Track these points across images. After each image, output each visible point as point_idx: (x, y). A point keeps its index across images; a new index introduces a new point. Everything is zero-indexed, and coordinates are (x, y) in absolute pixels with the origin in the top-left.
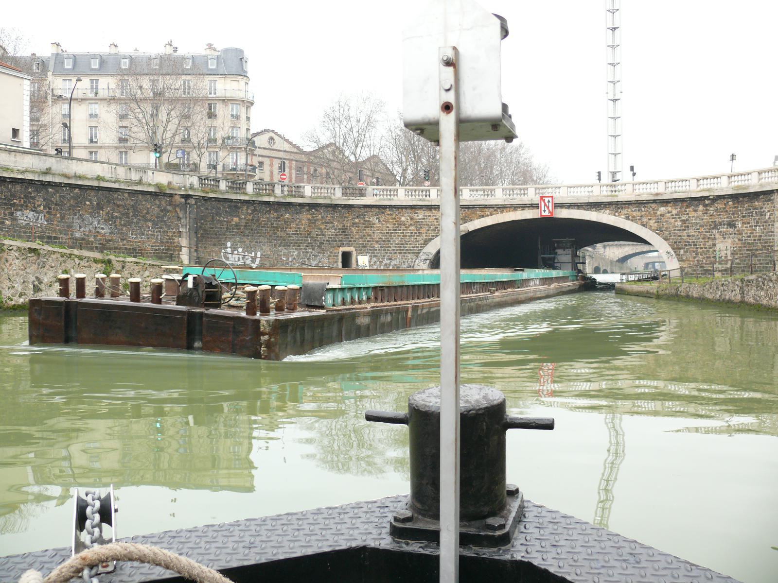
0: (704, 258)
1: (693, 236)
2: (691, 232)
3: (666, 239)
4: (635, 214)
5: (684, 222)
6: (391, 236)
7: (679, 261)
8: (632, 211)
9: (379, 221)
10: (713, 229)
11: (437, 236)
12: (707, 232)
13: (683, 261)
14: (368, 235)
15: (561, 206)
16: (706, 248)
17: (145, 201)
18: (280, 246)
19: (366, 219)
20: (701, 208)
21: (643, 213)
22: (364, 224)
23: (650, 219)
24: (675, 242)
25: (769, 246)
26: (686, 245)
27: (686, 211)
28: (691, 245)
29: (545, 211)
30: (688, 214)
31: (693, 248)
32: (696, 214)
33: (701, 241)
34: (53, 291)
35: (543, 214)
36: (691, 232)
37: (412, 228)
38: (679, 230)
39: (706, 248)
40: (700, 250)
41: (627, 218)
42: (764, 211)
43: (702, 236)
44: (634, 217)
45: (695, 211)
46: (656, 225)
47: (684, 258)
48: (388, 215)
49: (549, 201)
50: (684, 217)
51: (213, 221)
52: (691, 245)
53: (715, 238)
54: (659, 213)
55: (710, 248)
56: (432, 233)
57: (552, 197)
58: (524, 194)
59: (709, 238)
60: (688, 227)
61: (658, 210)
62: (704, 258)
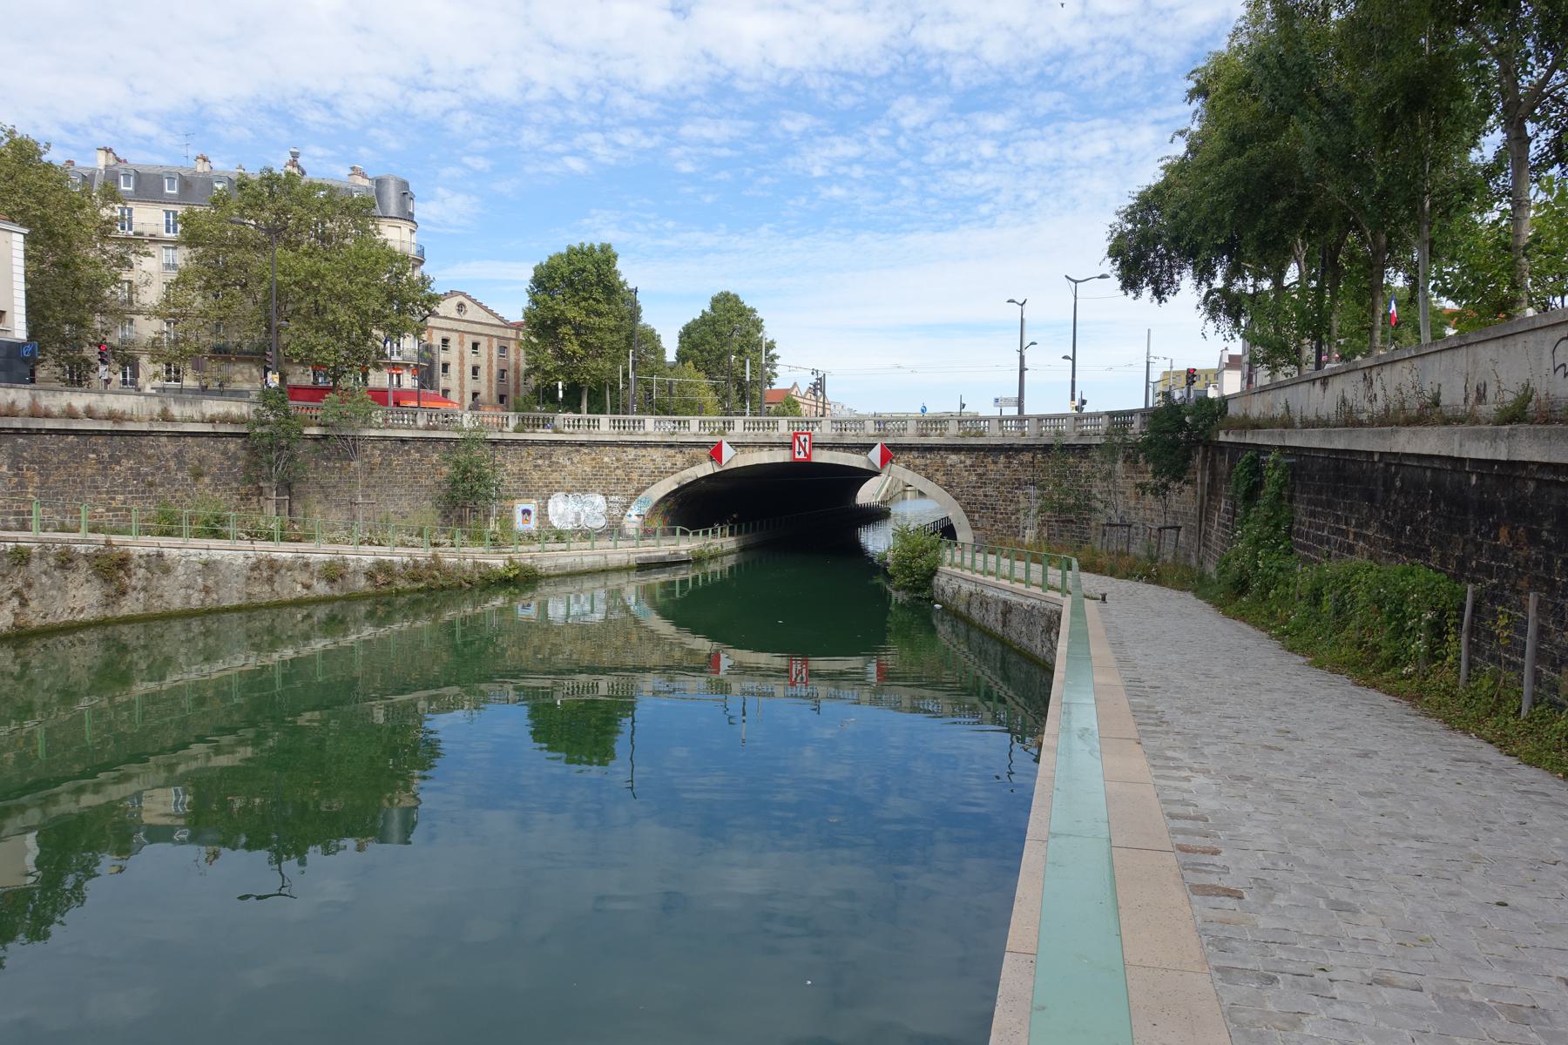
0: (1004, 527)
1: (991, 496)
2: (989, 490)
3: (956, 499)
4: (917, 462)
5: (979, 475)
6: (589, 483)
7: (973, 529)
8: (914, 458)
9: (572, 463)
10: (1017, 488)
11: (653, 484)
12: (1009, 492)
13: (978, 529)
14: (557, 482)
15: (822, 446)
16: (1007, 514)
17: (198, 446)
18: (425, 499)
19: (553, 459)
20: (1002, 459)
21: (928, 462)
22: (549, 467)
23: (937, 470)
24: (968, 503)
25: (1085, 519)
26: (982, 508)
27: (983, 462)
28: (988, 508)
29: (799, 453)
30: (985, 466)
31: (990, 513)
32: (997, 468)
33: (1001, 505)
34: (6, 612)
35: (797, 456)
36: (989, 490)
37: (619, 472)
38: (974, 487)
39: (1007, 514)
40: (999, 516)
41: (908, 467)
42: (1080, 471)
43: (1003, 498)
44: (916, 466)
45: (995, 463)
46: (944, 478)
47: (979, 525)
48: (585, 454)
49: (805, 440)
50: (980, 471)
51: (316, 468)
52: (988, 508)
53: (1019, 502)
54: (948, 462)
55: (1013, 514)
56: (647, 480)
57: (810, 434)
58: (774, 429)
59: (1011, 501)
60: (985, 483)
61: (947, 458)
62: (1004, 527)
